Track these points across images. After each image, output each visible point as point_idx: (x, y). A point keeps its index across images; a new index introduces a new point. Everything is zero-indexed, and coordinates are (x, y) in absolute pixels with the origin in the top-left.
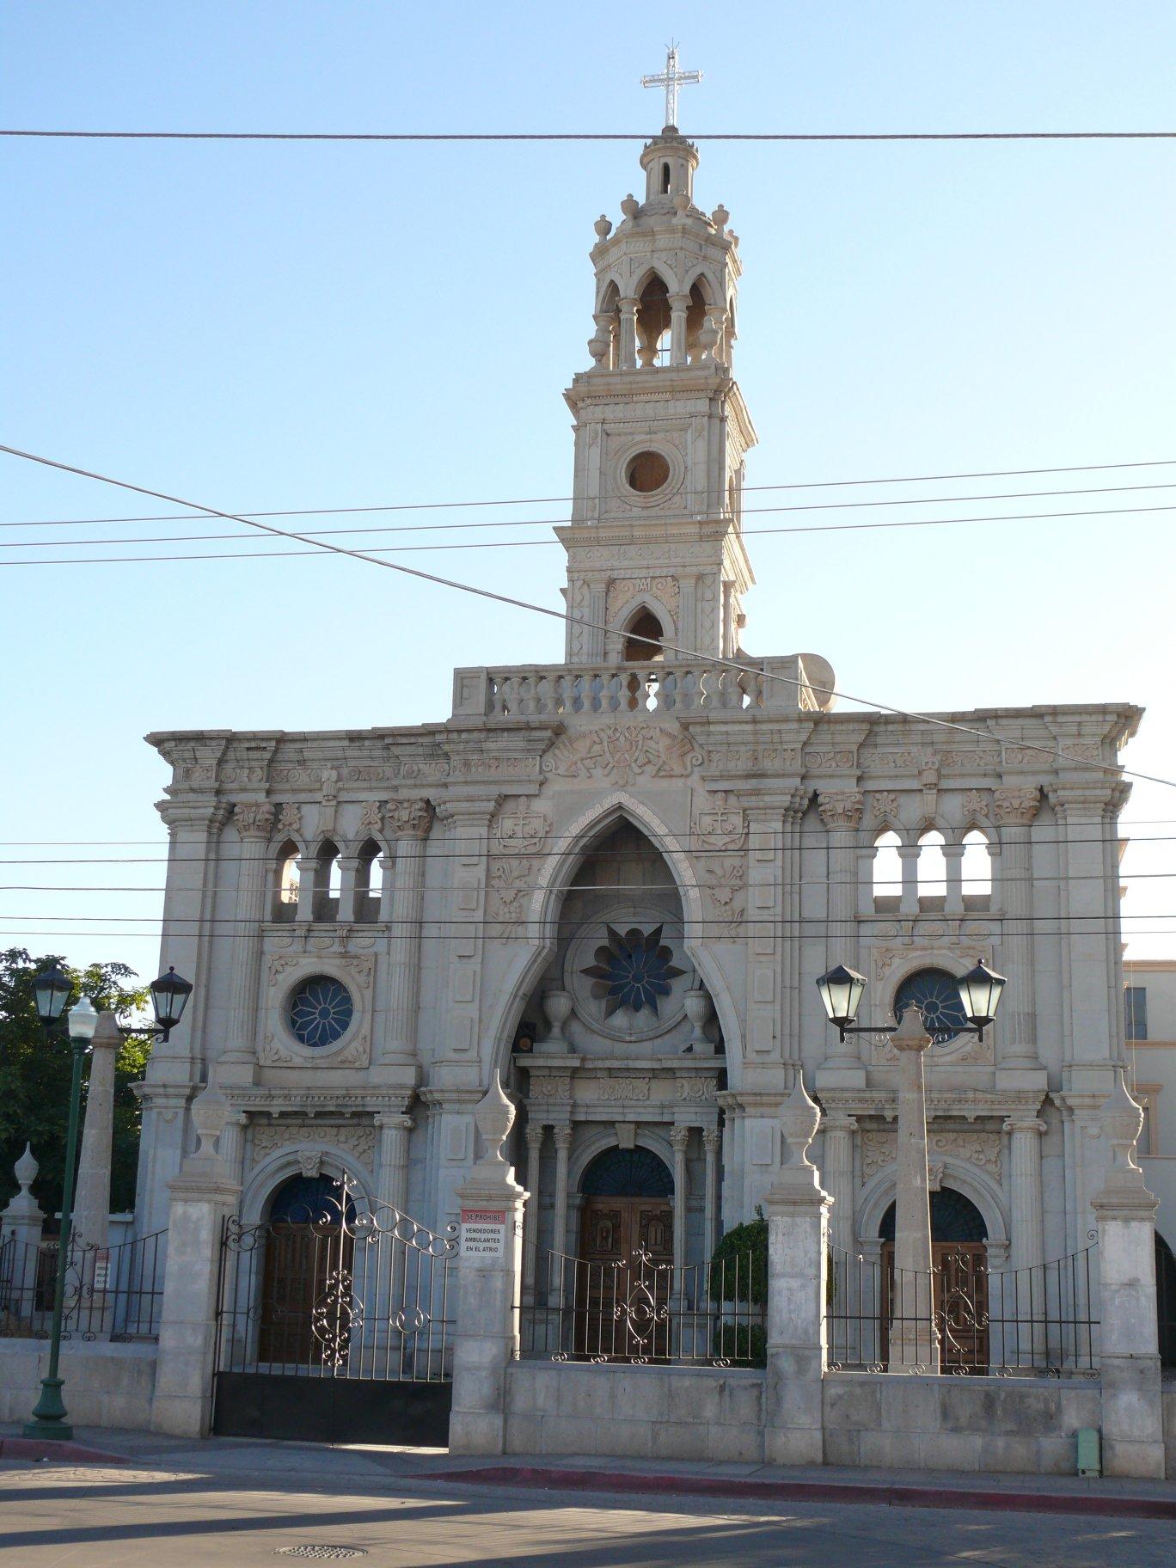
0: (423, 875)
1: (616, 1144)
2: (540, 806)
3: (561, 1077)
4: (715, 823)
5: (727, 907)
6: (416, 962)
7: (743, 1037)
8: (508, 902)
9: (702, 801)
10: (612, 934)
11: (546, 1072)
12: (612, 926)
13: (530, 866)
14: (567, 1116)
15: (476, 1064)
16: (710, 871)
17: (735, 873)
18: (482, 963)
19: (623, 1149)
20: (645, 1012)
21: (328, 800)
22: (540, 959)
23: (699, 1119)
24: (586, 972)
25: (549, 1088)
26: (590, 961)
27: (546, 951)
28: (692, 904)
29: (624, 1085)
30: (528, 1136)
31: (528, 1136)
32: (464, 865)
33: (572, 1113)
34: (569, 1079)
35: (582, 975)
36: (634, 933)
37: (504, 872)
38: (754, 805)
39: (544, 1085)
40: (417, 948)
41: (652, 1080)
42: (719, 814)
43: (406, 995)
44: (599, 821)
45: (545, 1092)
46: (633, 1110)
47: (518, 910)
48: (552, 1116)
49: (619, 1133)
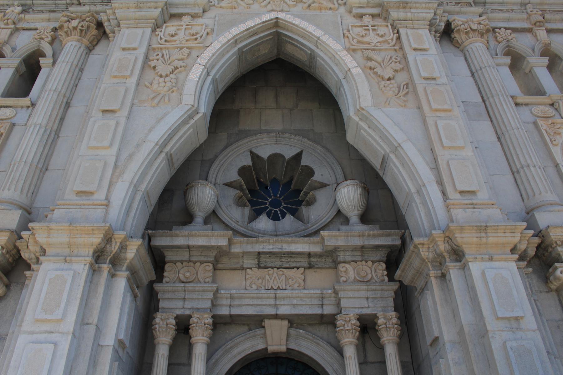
0: (81, 70)
1: (265, 347)
2: (200, 21)
3: (202, 263)
4: (367, 32)
5: (392, 81)
6: (55, 128)
7: (440, 183)
8: (164, 74)
9: (350, 20)
10: (254, 156)
11: (185, 256)
12: (254, 151)
13: (190, 52)
14: (208, 304)
15: (105, 207)
16: (369, 59)
17: (393, 59)
18: (128, 118)
19: (274, 353)
20: (288, 221)
21: (7, 24)
22: (192, 122)
23: (371, 305)
24: (229, 185)
25: (188, 274)
26: (234, 176)
27: (199, 115)
28: (356, 78)
29: (275, 275)
30: (157, 326)
31: (157, 326)
32: (124, 49)
33: (214, 305)
34: (211, 265)
35: (226, 187)
36: (275, 158)
37: (163, 56)
38: (402, 15)
39: (181, 271)
40: (59, 118)
41: (307, 271)
42: (370, 26)
43: (34, 150)
44: (255, 34)
45: (181, 275)
46: (286, 302)
47: (174, 81)
48: (188, 305)
49: (268, 333)
